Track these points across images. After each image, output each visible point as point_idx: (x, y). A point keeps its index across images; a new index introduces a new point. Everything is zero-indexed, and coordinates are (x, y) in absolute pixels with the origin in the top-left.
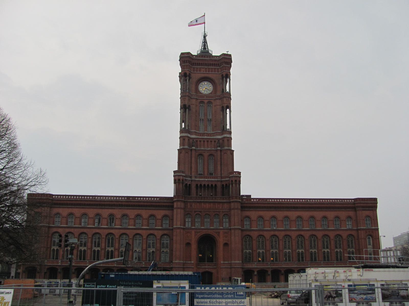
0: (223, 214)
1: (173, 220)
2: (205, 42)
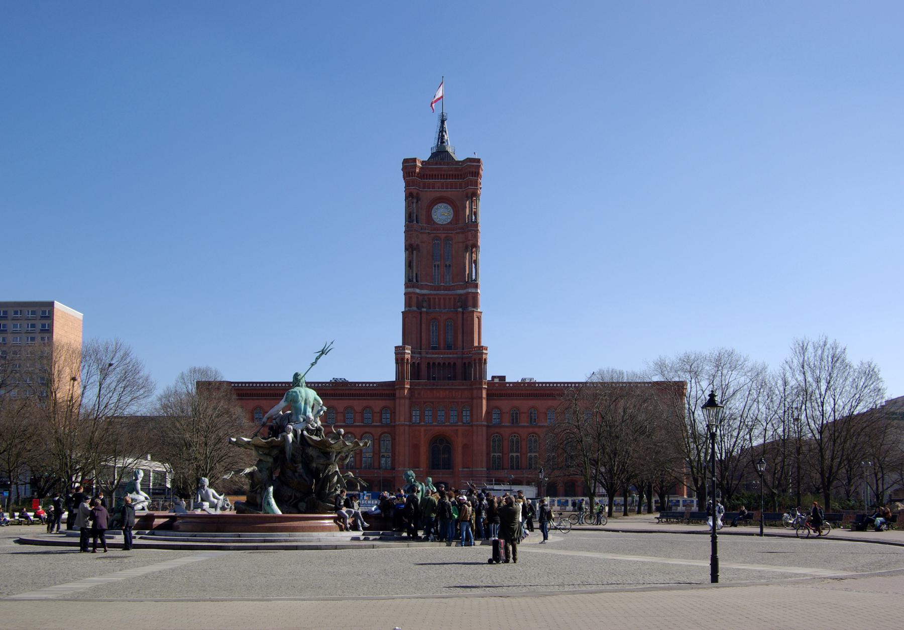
1: (395, 413)
2: (442, 130)
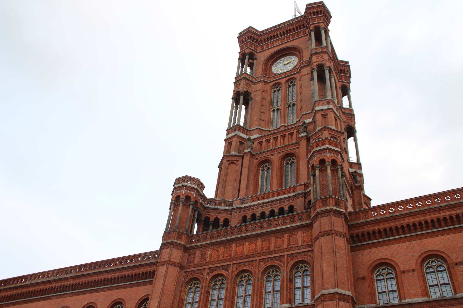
0: (292, 263)
